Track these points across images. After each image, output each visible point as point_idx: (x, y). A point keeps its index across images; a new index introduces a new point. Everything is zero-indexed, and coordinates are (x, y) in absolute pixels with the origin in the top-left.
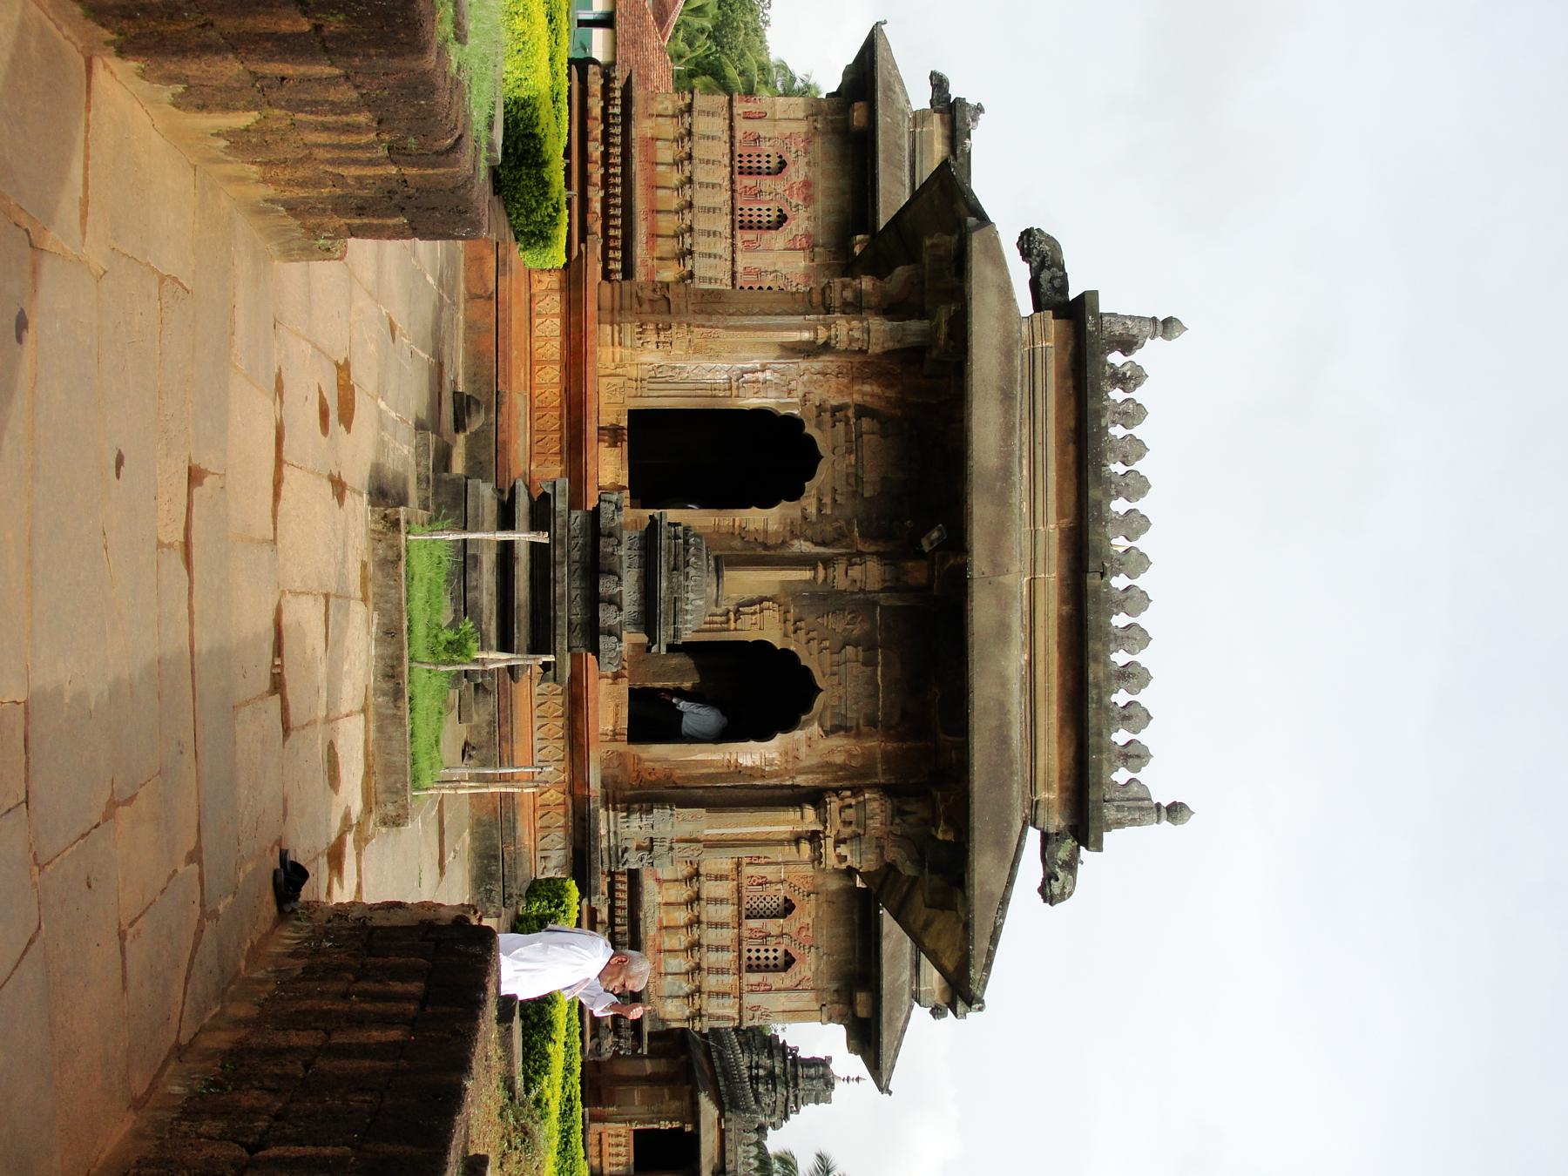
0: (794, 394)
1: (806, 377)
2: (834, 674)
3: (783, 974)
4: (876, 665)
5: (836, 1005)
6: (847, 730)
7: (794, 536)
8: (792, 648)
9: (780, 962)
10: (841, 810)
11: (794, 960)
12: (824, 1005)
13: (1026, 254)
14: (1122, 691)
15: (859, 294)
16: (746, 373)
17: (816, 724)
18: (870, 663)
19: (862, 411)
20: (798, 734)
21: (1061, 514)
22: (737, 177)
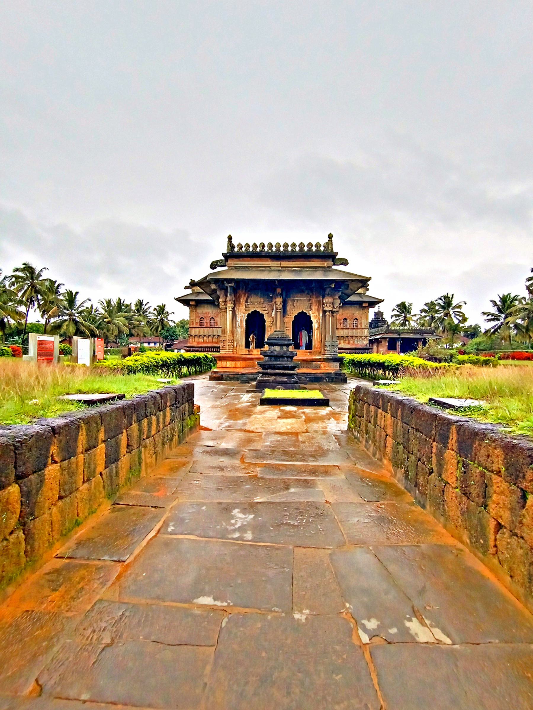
4: (297, 300)
6: (310, 306)
13: (215, 268)
15: (223, 302)
19: (246, 302)
20: (311, 316)
21: (268, 261)
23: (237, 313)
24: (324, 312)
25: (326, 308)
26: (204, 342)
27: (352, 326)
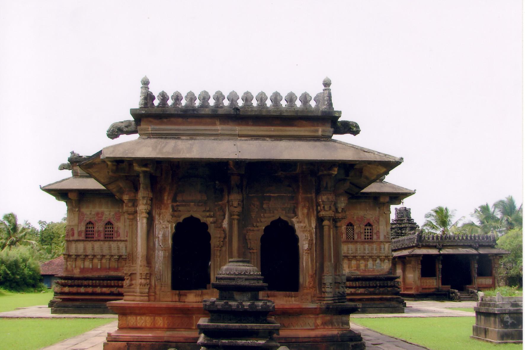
0: (167, 226)
1: (161, 221)
2: (273, 213)
3: (374, 227)
4: (270, 197)
7: (221, 227)
8: (264, 228)
9: (369, 228)
10: (324, 210)
11: (369, 223)
12: (384, 213)
15: (130, 200)
16: (159, 244)
18: (269, 198)
19: (174, 200)
20: (296, 226)
21: (214, 124)
22: (95, 239)
23: (157, 222)
24: (320, 220)
25: (322, 213)
26: (93, 269)
27: (363, 237)
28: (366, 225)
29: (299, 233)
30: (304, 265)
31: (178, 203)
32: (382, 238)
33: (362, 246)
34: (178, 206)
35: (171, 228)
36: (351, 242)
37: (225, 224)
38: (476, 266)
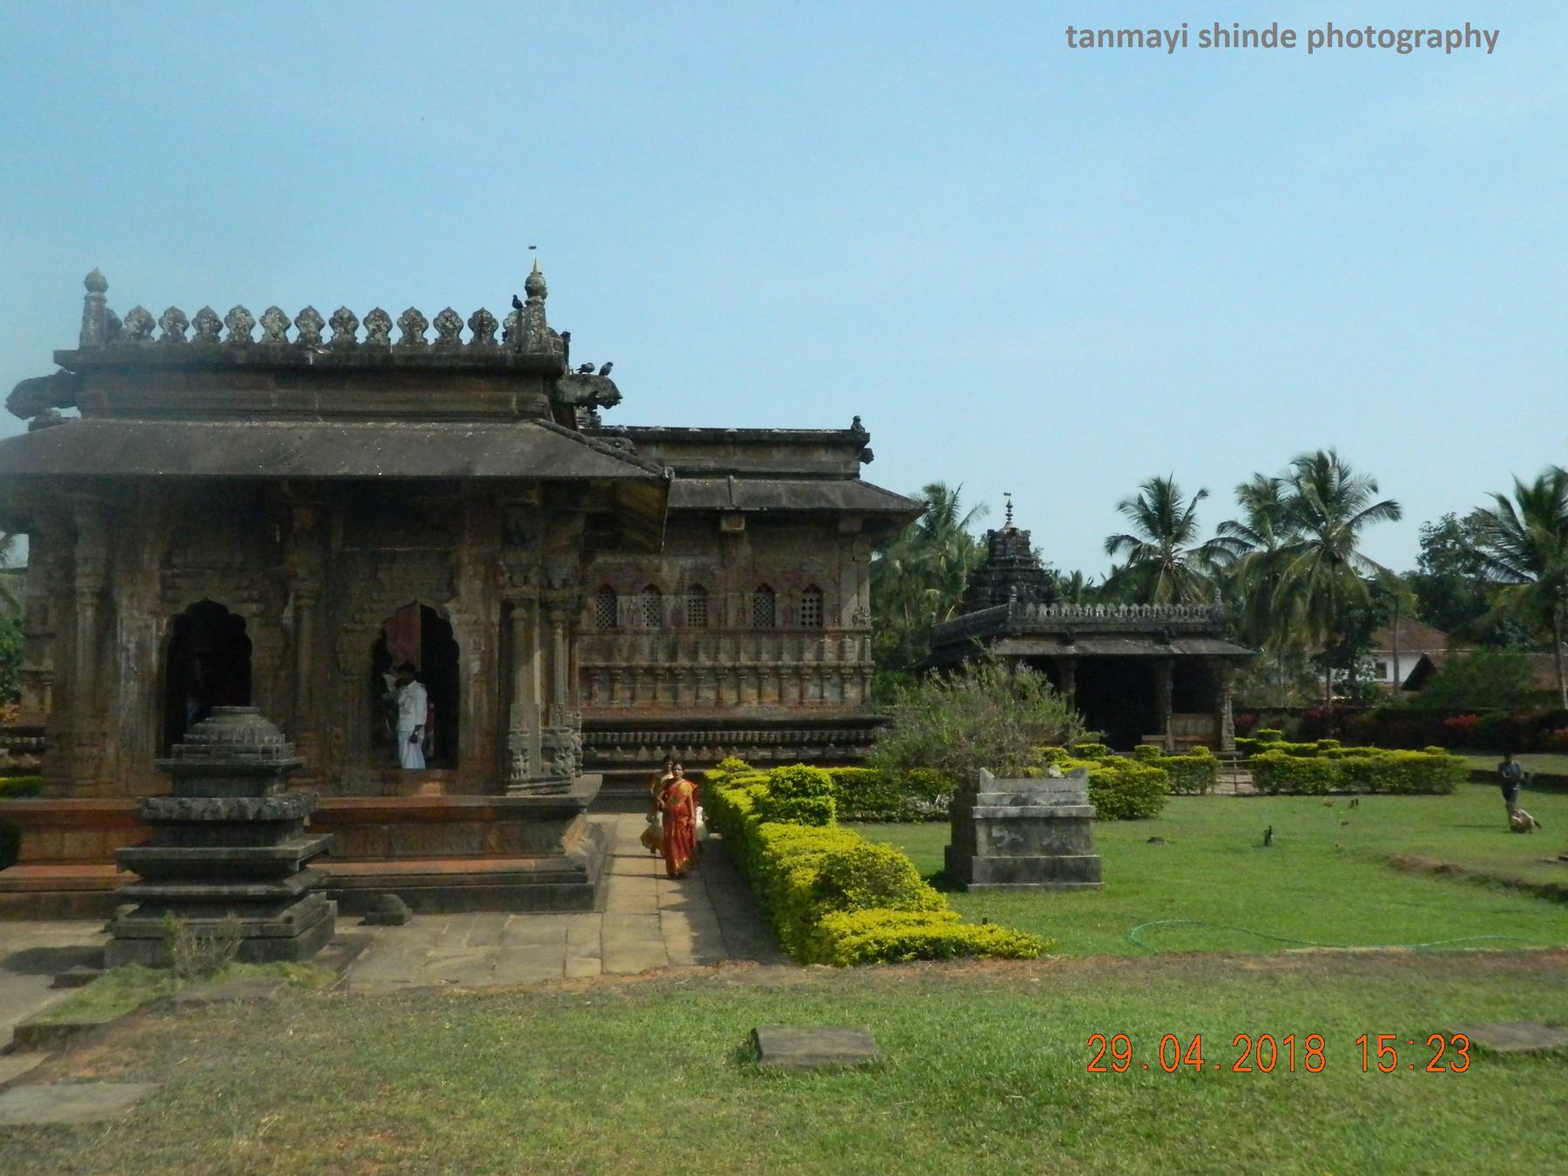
3: (825, 594)
5: (854, 548)
6: (452, 578)
7: (278, 623)
9: (814, 596)
11: (812, 585)
14: (426, 335)
17: (446, 605)
19: (166, 562)
20: (454, 620)
23: (123, 613)
24: (507, 606)
25: (509, 592)
27: (797, 619)
28: (807, 591)
29: (459, 635)
30: (471, 709)
31: (176, 571)
32: (847, 623)
33: (796, 642)
34: (175, 576)
35: (159, 628)
36: (768, 633)
37: (288, 614)
38: (1169, 686)
